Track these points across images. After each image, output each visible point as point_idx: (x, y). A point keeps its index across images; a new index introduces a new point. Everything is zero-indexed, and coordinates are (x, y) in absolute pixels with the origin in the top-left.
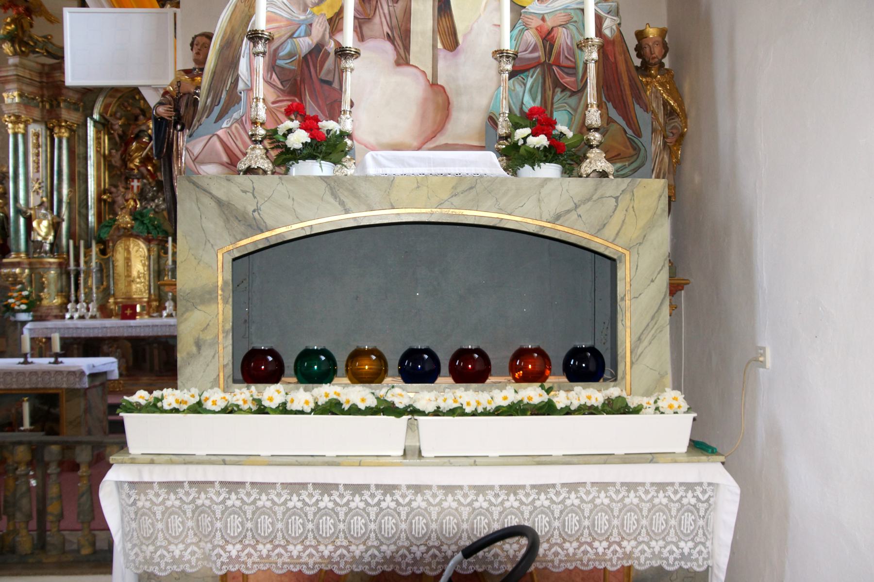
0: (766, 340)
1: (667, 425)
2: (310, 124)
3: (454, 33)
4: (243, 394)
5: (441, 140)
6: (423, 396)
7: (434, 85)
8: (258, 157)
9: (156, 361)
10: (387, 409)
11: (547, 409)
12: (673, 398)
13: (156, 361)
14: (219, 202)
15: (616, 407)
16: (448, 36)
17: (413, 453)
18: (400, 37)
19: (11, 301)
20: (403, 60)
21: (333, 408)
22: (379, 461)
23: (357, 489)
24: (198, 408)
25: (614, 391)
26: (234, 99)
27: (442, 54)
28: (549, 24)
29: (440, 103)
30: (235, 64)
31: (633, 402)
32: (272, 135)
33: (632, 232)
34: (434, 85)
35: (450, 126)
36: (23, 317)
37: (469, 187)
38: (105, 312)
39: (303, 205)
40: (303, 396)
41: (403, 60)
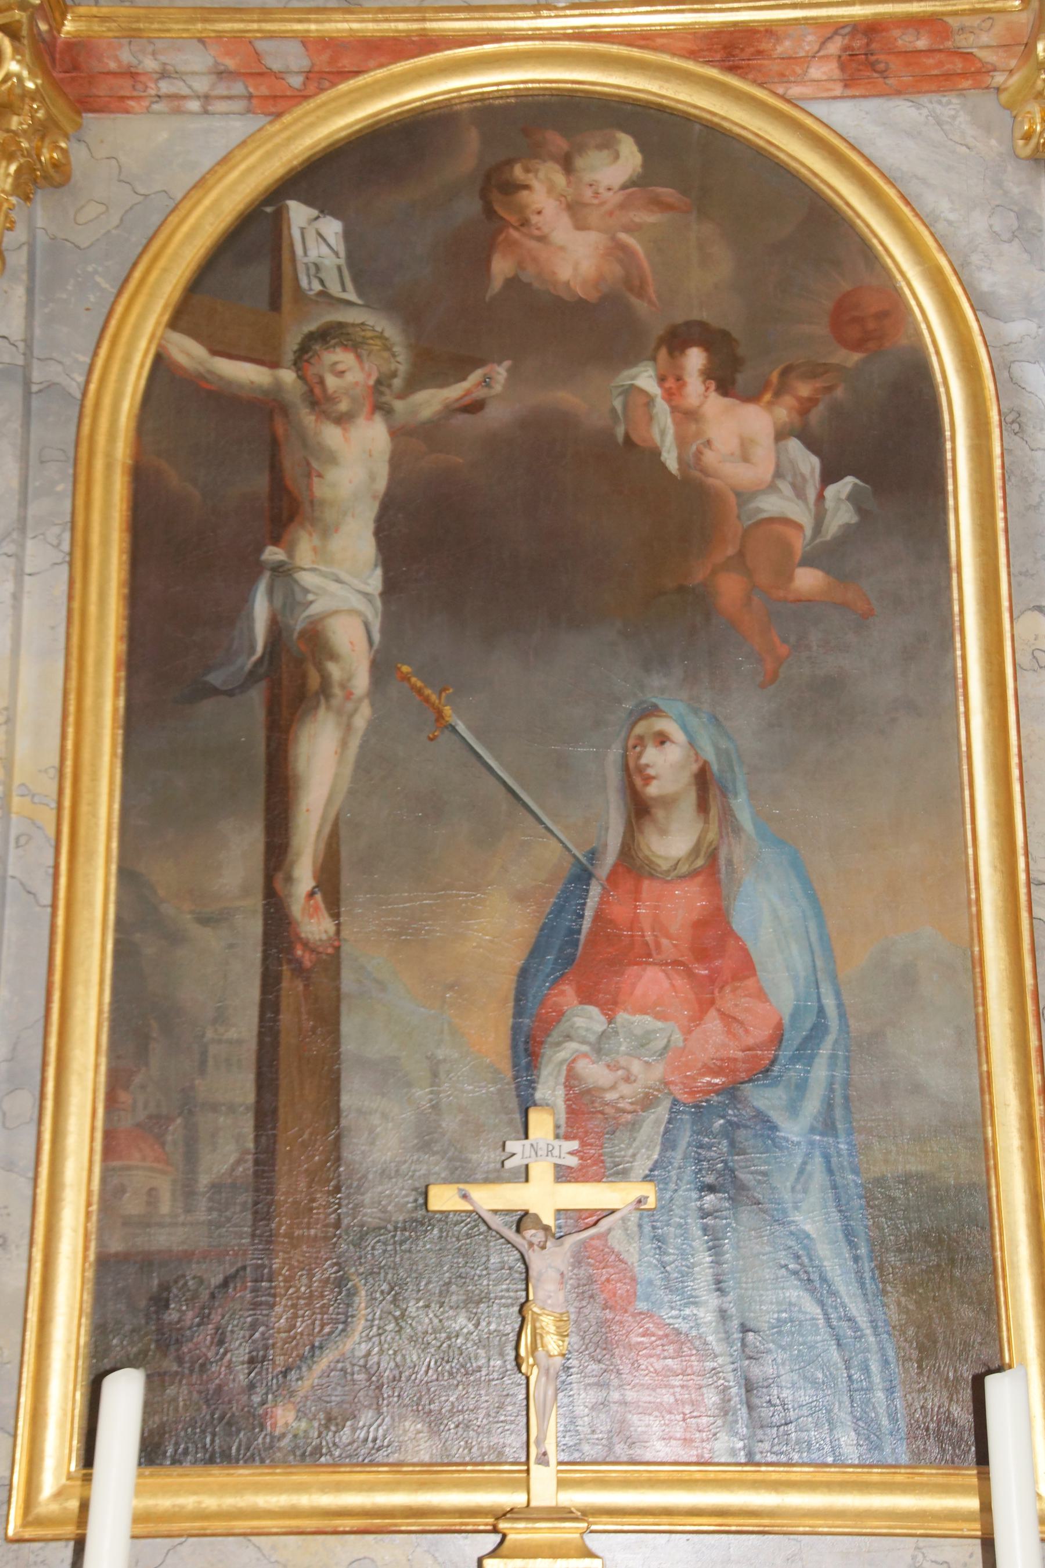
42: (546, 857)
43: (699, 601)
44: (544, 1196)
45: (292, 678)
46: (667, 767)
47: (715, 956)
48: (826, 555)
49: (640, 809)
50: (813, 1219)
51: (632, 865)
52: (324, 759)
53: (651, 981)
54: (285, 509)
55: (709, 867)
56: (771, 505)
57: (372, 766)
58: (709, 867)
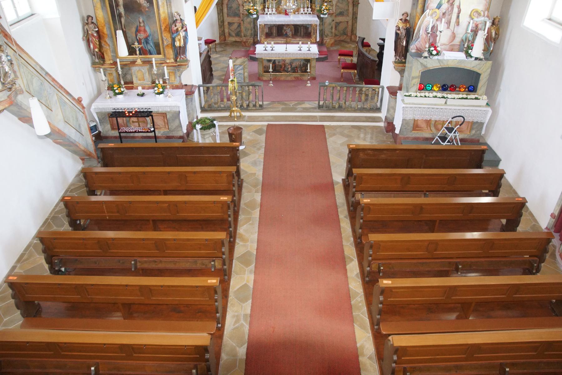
0: (502, 88)
1: (484, 100)
2: (435, 49)
3: (459, 22)
4: (423, 94)
5: (452, 43)
6: (449, 96)
7: (453, 33)
8: (426, 54)
9: (302, 33)
10: (443, 97)
11: (466, 98)
12: (485, 97)
13: (302, 33)
14: (421, 63)
15: (476, 99)
16: (458, 23)
17: (446, 103)
18: (449, 23)
19: (251, 11)
20: (448, 28)
21: (436, 97)
22: (441, 105)
23: (437, 109)
24: (416, 96)
25: (477, 96)
26: (419, 37)
27: (456, 26)
28: (478, 23)
29: (454, 36)
30: (419, 31)
31: (479, 97)
32: (429, 50)
33: (485, 70)
34: (453, 33)
35: (454, 41)
36: (255, 16)
37: (461, 61)
38: (280, 13)
39: (433, 63)
40: (431, 95)
41: (448, 28)
42: (136, 26)
43: (141, 11)
44: (137, 46)
45: (120, 16)
46: (141, 20)
47: (145, 31)
48: (148, 8)
49: (140, 23)
50: (151, 44)
51: (140, 26)
52: (123, 20)
53: (142, 32)
54: (117, 5)
55: (144, 26)
56: (145, 5)
57: (126, 21)
58: (144, 26)
